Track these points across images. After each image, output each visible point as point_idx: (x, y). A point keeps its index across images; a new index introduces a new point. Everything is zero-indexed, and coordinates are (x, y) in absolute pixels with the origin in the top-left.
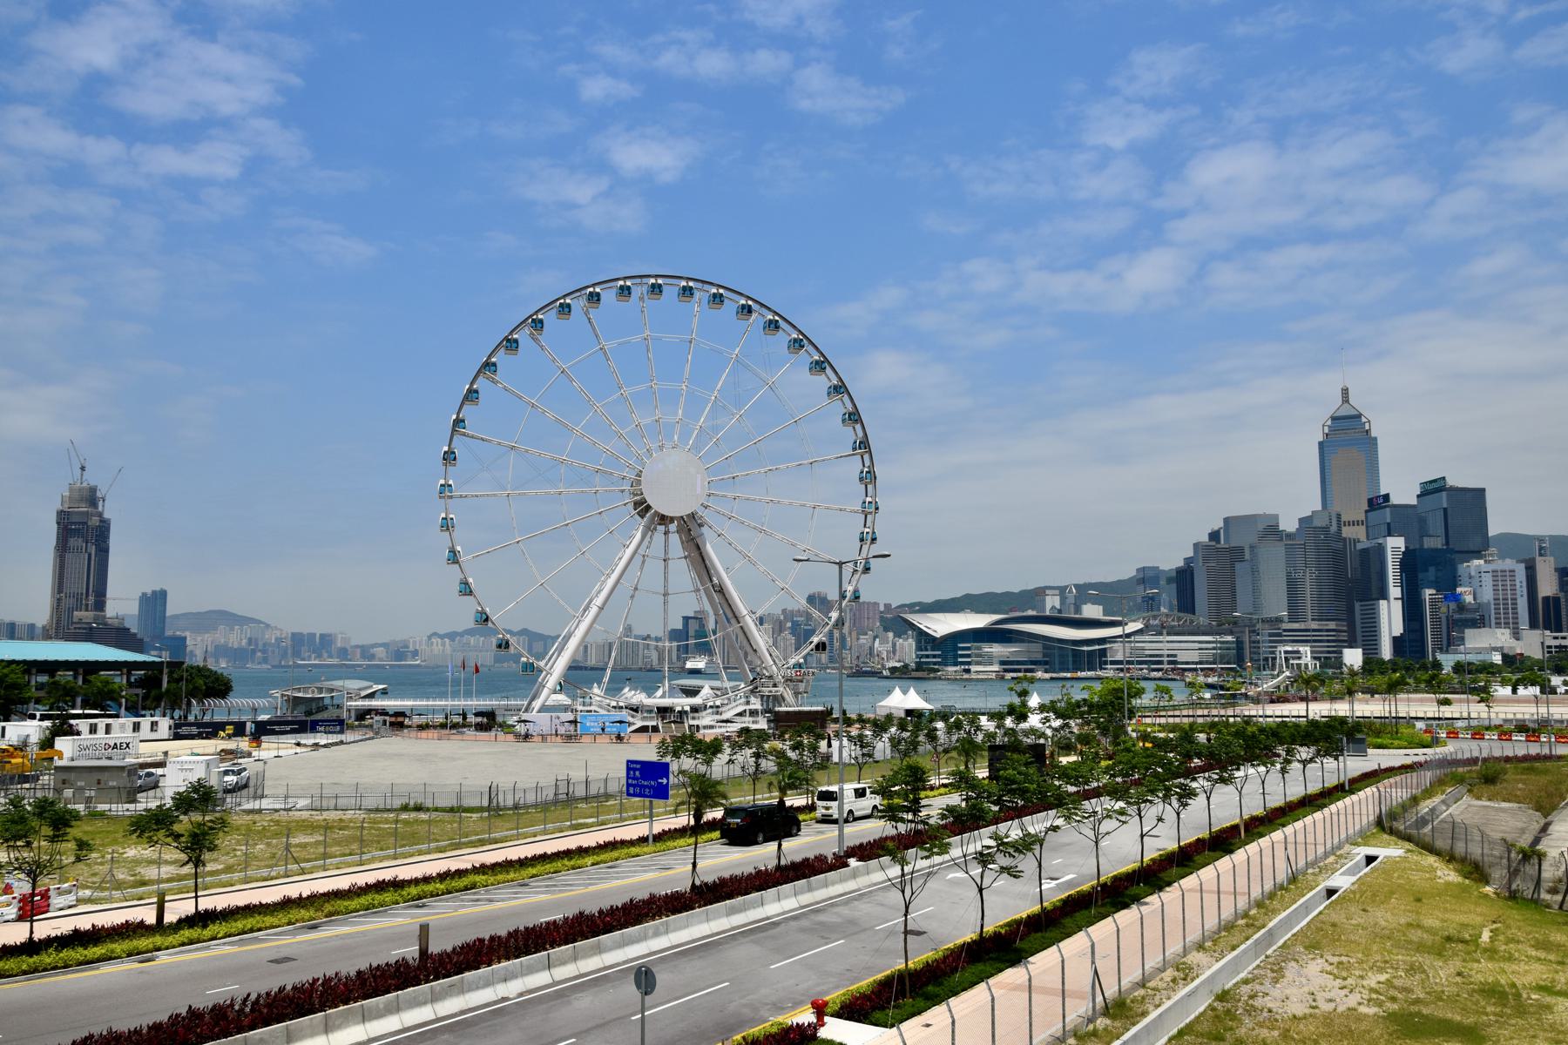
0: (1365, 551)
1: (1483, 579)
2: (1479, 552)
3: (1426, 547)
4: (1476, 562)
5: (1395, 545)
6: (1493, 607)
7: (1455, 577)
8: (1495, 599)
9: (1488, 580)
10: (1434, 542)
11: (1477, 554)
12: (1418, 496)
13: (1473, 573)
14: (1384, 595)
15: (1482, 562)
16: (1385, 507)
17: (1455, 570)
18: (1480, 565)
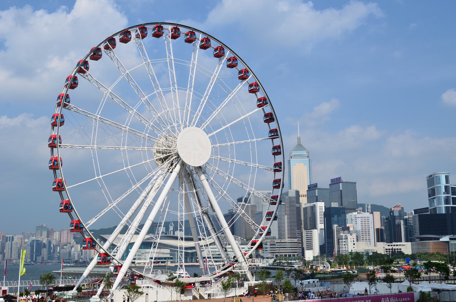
0: (305, 209)
1: (357, 220)
2: (355, 209)
3: (332, 206)
4: (355, 213)
5: (320, 206)
6: (361, 232)
7: (345, 220)
8: (362, 229)
9: (359, 221)
10: (335, 205)
11: (354, 210)
12: (330, 185)
13: (353, 218)
14: (314, 226)
15: (356, 213)
16: (316, 189)
17: (346, 217)
18: (355, 215)
